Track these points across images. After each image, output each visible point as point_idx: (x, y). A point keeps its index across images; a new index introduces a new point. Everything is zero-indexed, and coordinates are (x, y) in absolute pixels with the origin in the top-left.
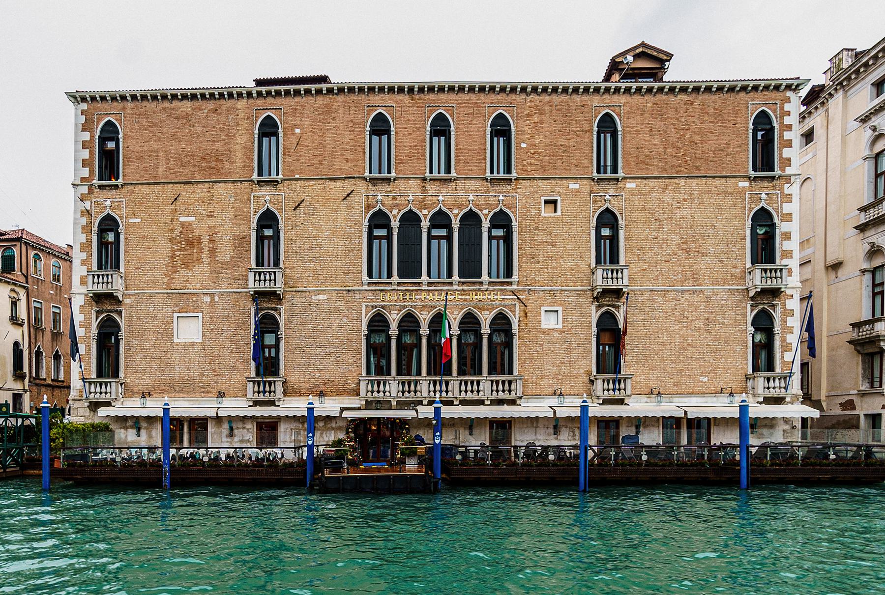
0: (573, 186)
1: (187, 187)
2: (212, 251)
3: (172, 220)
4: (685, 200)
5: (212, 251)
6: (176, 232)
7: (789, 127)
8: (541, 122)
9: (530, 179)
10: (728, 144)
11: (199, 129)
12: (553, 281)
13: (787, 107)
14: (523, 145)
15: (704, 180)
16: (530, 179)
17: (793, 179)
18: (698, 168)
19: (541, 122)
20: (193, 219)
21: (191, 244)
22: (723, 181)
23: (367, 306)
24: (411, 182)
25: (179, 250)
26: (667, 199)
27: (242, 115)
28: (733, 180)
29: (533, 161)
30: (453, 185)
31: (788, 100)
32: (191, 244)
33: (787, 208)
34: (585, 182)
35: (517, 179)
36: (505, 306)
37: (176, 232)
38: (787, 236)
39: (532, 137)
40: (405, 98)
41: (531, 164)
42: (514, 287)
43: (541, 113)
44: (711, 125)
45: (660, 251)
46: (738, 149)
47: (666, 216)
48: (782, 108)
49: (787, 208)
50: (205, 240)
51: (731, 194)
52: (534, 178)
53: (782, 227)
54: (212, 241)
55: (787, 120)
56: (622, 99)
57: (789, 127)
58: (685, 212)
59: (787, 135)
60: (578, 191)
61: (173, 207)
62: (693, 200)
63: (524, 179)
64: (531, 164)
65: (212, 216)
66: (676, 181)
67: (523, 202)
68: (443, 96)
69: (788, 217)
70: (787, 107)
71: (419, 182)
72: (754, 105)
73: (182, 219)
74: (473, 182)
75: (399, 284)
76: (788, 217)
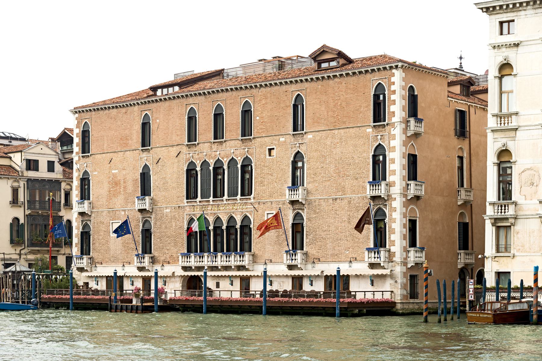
0: (282, 139)
1: (115, 154)
2: (125, 187)
3: (109, 172)
4: (337, 143)
5: (125, 187)
6: (111, 179)
7: (394, 92)
8: (266, 103)
9: (260, 137)
10: (360, 106)
11: (119, 123)
12: (271, 196)
13: (393, 79)
14: (258, 118)
15: (348, 129)
16: (260, 137)
17: (396, 124)
18: (344, 123)
19: (266, 103)
20: (117, 171)
21: (116, 184)
22: (358, 129)
23: (187, 215)
24: (206, 144)
25: (112, 188)
26: (329, 143)
27: (136, 115)
28: (363, 128)
29: (262, 127)
30: (224, 144)
31: (393, 75)
32: (116, 184)
33: (393, 143)
34: (287, 136)
35: (254, 138)
36: (247, 212)
37: (111, 179)
38: (393, 161)
39: (262, 113)
40: (203, 98)
41: (261, 129)
42: (252, 200)
43: (266, 98)
44: (352, 95)
45: (324, 175)
46: (366, 109)
47: (328, 154)
48: (389, 80)
49: (393, 143)
50: (122, 182)
51: (363, 137)
52: (262, 137)
53: (390, 156)
54: (124, 182)
55: (393, 88)
56: (306, 85)
57: (394, 92)
58: (338, 150)
59: (393, 97)
60: (285, 142)
61: (109, 165)
62: (342, 142)
63: (258, 137)
64: (261, 129)
65: (124, 169)
66: (333, 131)
67: (256, 151)
68: (221, 94)
69: (393, 149)
70: (393, 79)
71: (209, 144)
72: (374, 80)
73: (113, 171)
74: (233, 141)
75: (200, 202)
76: (393, 149)
